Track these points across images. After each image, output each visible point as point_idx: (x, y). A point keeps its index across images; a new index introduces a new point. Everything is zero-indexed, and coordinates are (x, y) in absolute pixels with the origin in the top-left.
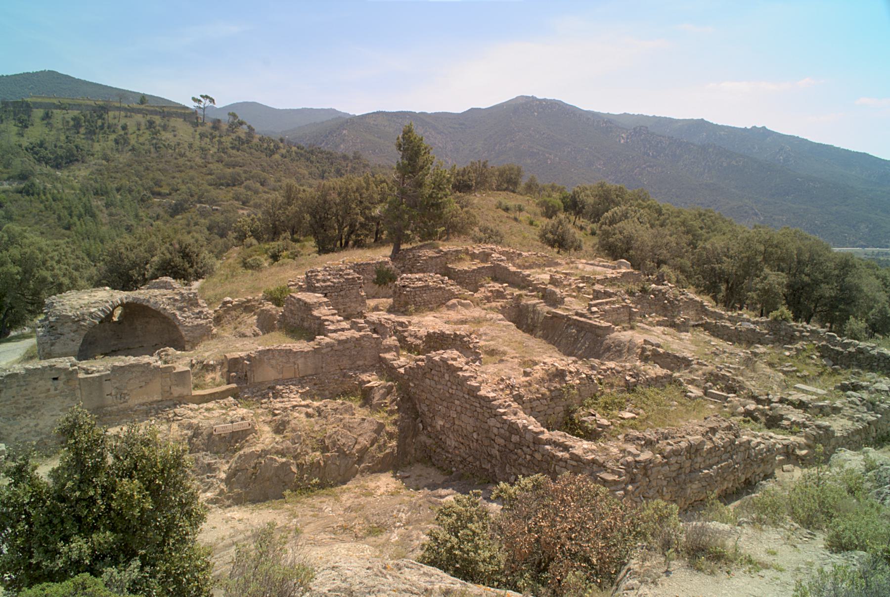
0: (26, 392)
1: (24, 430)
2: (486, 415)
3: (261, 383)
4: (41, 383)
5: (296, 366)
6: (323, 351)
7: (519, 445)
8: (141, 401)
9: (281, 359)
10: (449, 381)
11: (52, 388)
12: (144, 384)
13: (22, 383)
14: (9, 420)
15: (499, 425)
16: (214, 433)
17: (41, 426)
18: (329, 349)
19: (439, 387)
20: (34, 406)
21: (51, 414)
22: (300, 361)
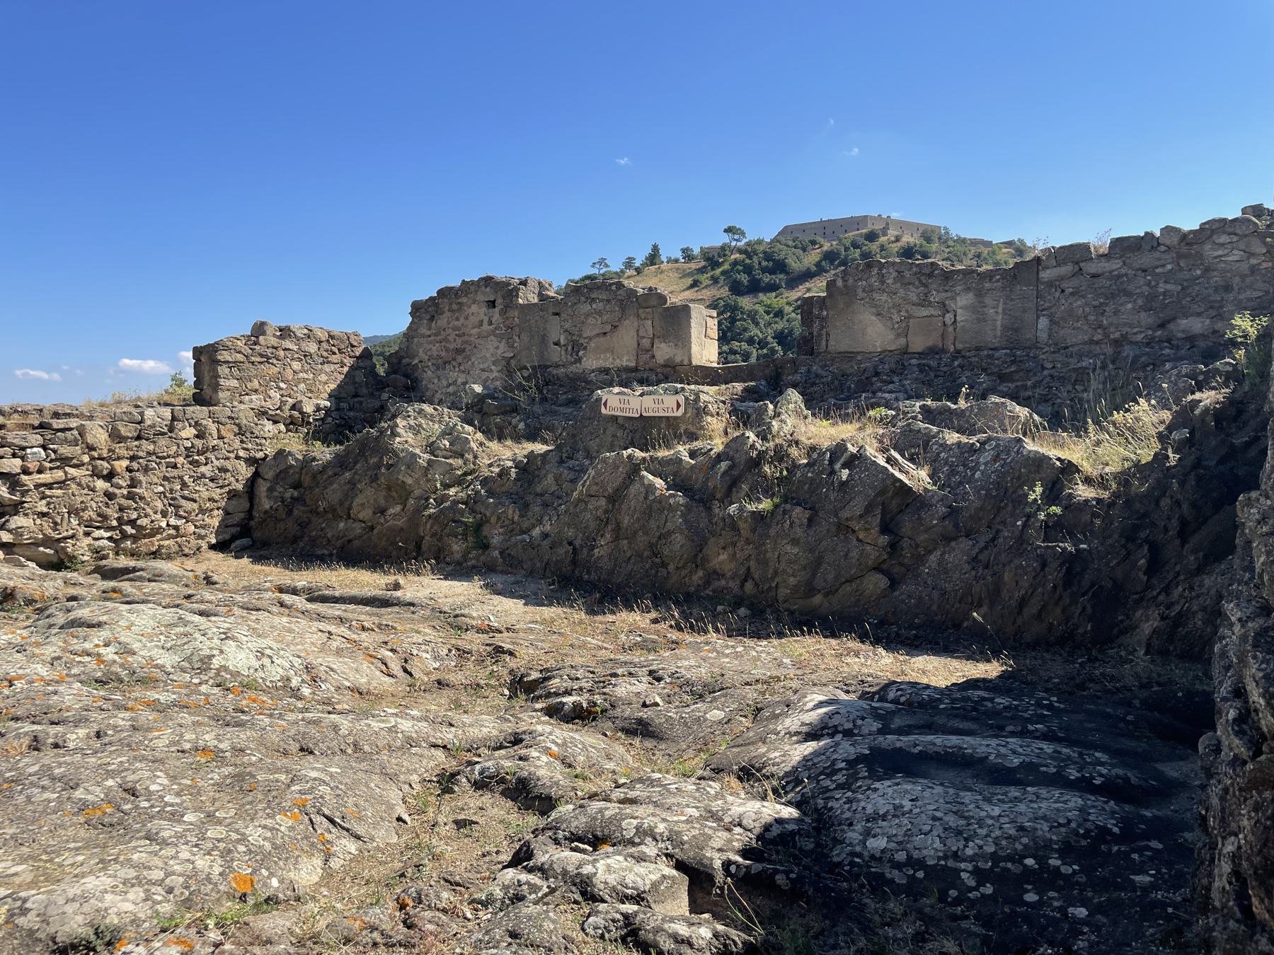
0: (456, 323)
3: (849, 356)
6: (1046, 275)
11: (486, 320)
12: (608, 328)
13: (455, 307)
14: (438, 368)
16: (603, 411)
20: (464, 350)
21: (481, 366)
22: (964, 301)
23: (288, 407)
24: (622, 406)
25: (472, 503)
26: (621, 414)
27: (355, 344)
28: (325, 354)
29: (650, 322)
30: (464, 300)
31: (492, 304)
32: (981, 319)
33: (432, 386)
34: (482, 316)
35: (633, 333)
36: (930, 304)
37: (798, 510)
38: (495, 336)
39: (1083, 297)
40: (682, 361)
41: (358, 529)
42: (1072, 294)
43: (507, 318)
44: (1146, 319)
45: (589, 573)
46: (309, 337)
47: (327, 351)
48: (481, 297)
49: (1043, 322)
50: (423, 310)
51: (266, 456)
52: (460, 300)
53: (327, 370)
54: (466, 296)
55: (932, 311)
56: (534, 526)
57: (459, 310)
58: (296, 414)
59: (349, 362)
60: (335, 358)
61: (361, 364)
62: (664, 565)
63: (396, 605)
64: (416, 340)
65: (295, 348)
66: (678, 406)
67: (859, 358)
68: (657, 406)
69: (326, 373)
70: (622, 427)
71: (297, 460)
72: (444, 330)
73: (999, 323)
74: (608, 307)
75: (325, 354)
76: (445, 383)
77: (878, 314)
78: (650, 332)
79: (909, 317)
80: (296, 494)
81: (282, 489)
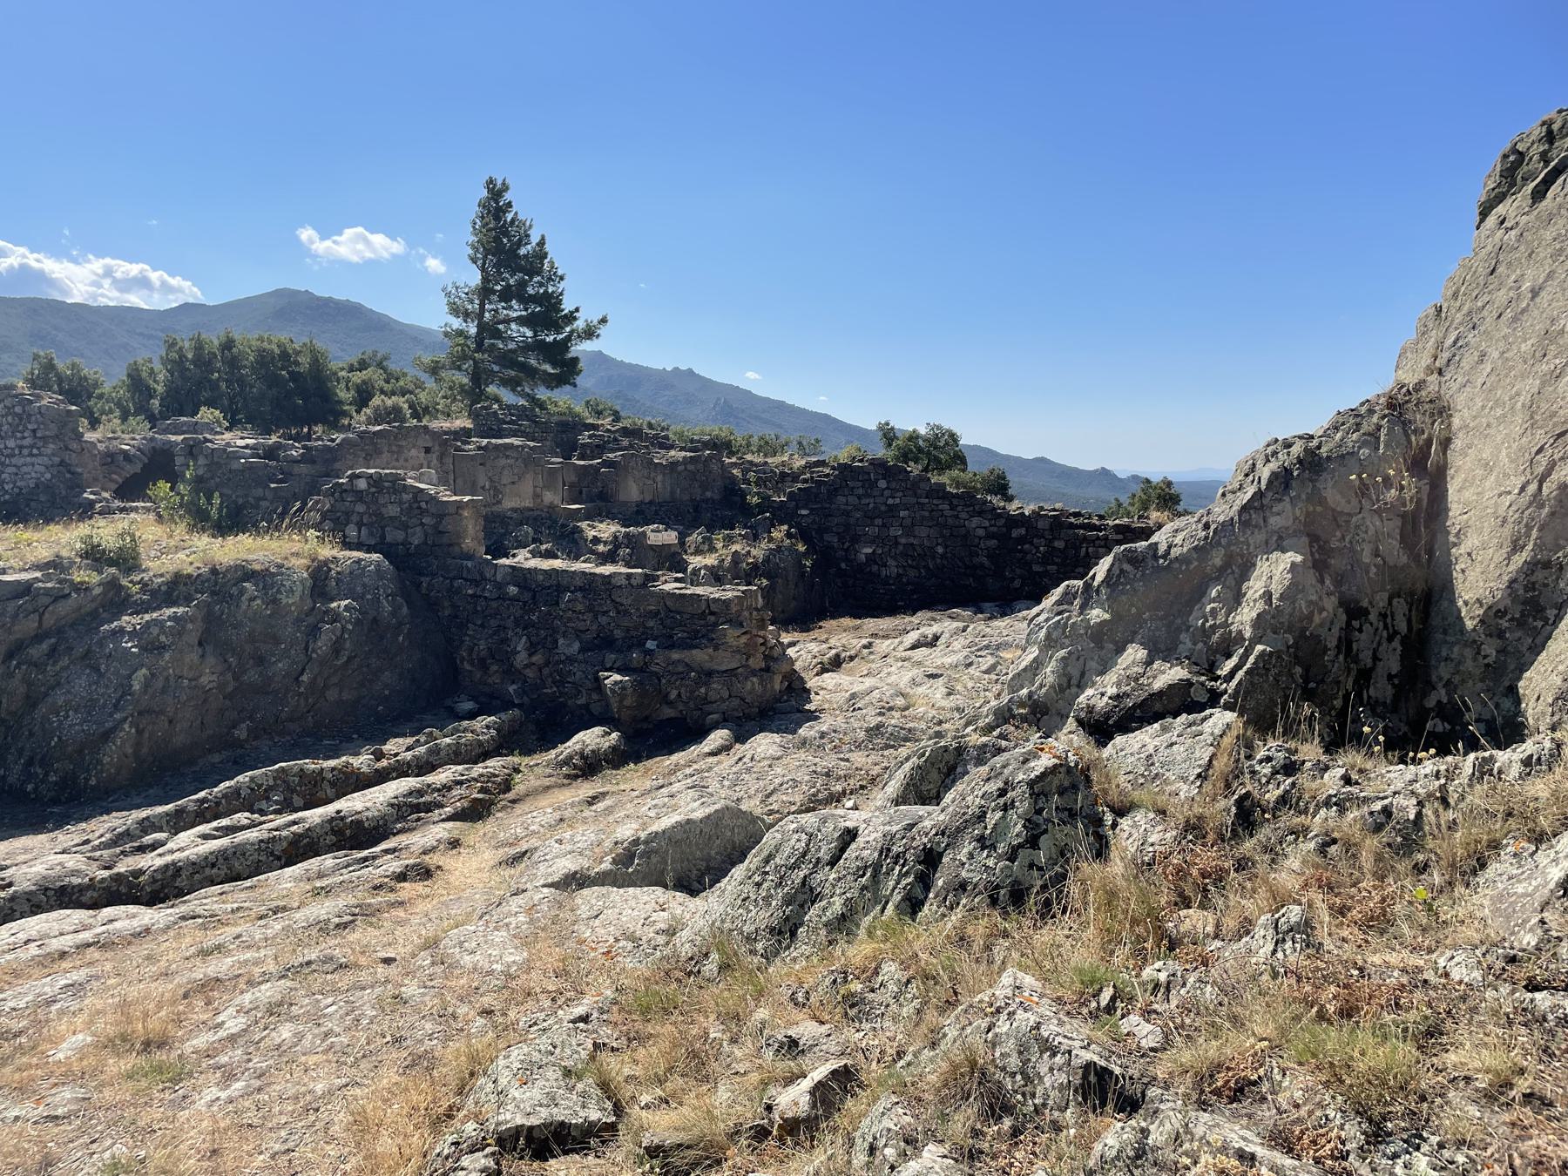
2: (964, 515)
6: (680, 468)
7: (1021, 540)
10: (887, 488)
13: (394, 448)
15: (987, 524)
19: (864, 501)
30: (404, 443)
48: (421, 443)
57: (399, 453)
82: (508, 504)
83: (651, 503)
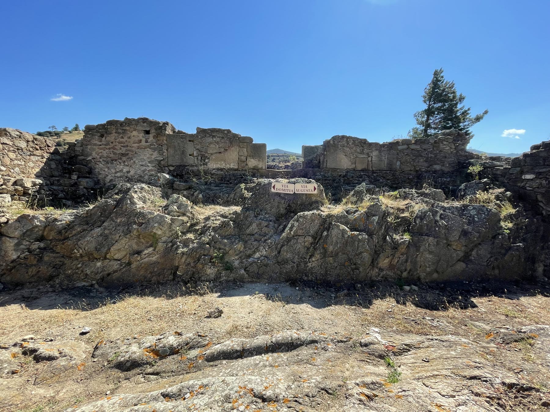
0: (121, 140)
1: (118, 174)
3: (335, 170)
4: (135, 133)
5: (370, 159)
6: (400, 148)
8: (218, 166)
9: (354, 148)
11: (144, 140)
12: (222, 150)
13: (120, 131)
14: (107, 163)
16: (272, 190)
17: (132, 173)
18: (405, 147)
20: (128, 154)
21: (141, 163)
22: (375, 153)
23: (11, 183)
24: (284, 188)
25: (213, 242)
26: (283, 192)
27: (50, 145)
28: (31, 149)
29: (245, 149)
30: (128, 128)
31: (148, 132)
32: (381, 160)
33: (103, 172)
34: (141, 138)
35: (236, 153)
36: (364, 154)
37: (431, 239)
38: (150, 148)
39: (409, 156)
40: (262, 167)
41: (115, 265)
42: (407, 155)
43: (158, 140)
44: (426, 164)
45: (306, 276)
46: (20, 137)
47: (32, 147)
49: (398, 163)
50: (95, 131)
51: (8, 220)
52: (124, 128)
53: (33, 160)
54: (128, 126)
55: (365, 156)
56: (254, 252)
58: (19, 188)
59: (46, 155)
60: (38, 152)
61: (54, 158)
62: (357, 269)
63: (301, 345)
64: (89, 147)
65: (11, 143)
66: (315, 189)
67: (338, 171)
68: (303, 188)
69: (33, 162)
70: (283, 198)
71: (41, 221)
72: (112, 143)
73: (386, 162)
74: (223, 141)
75: (31, 149)
76: (113, 171)
77: (346, 155)
78: (246, 154)
79: (357, 157)
80: (42, 245)
81: (28, 243)
82: (212, 165)
83: (363, 170)
